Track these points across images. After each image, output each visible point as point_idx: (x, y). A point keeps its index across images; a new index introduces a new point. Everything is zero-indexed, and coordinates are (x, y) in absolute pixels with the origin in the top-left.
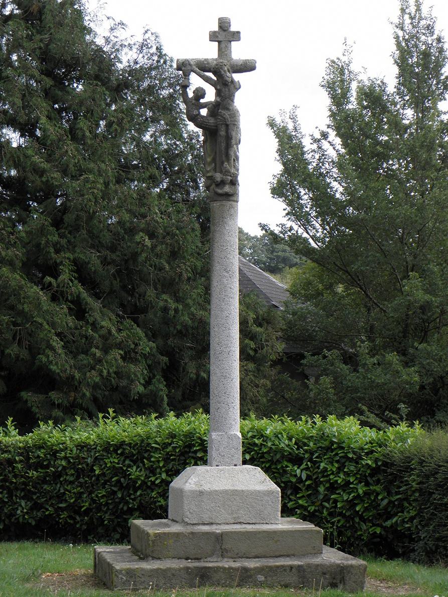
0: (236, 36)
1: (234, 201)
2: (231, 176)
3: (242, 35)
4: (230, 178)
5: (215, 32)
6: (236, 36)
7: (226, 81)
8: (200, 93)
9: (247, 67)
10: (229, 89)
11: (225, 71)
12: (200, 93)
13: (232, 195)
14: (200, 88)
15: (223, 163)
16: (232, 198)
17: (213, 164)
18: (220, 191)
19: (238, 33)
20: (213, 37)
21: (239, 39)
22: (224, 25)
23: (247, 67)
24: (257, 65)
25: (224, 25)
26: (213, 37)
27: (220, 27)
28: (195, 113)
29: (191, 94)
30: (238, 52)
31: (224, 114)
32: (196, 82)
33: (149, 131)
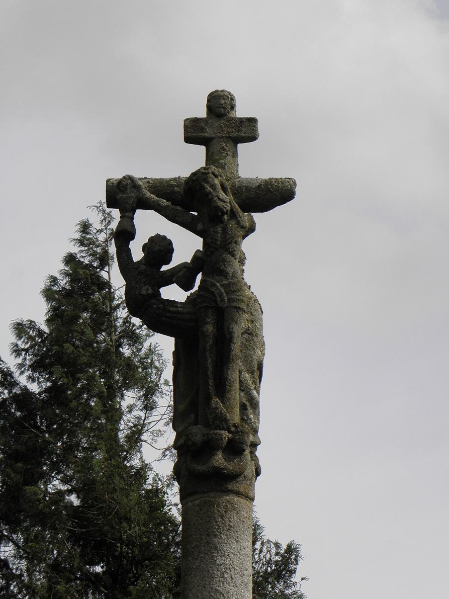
0: (247, 131)
1: (238, 493)
2: (230, 432)
3: (261, 127)
4: (226, 435)
5: (196, 120)
6: (247, 131)
7: (218, 208)
8: (160, 249)
9: (275, 194)
10: (225, 230)
11: (213, 186)
12: (160, 249)
13: (234, 477)
14: (158, 236)
15: (209, 399)
16: (231, 486)
17: (193, 416)
18: (201, 468)
19: (252, 121)
20: (194, 132)
21: (252, 137)
22: (219, 103)
23: (275, 194)
24: (297, 190)
25: (219, 103)
26: (194, 132)
27: (210, 108)
28: (144, 292)
29: (137, 254)
30: (252, 164)
31: (214, 285)
32: (149, 224)
33: (135, 437)
